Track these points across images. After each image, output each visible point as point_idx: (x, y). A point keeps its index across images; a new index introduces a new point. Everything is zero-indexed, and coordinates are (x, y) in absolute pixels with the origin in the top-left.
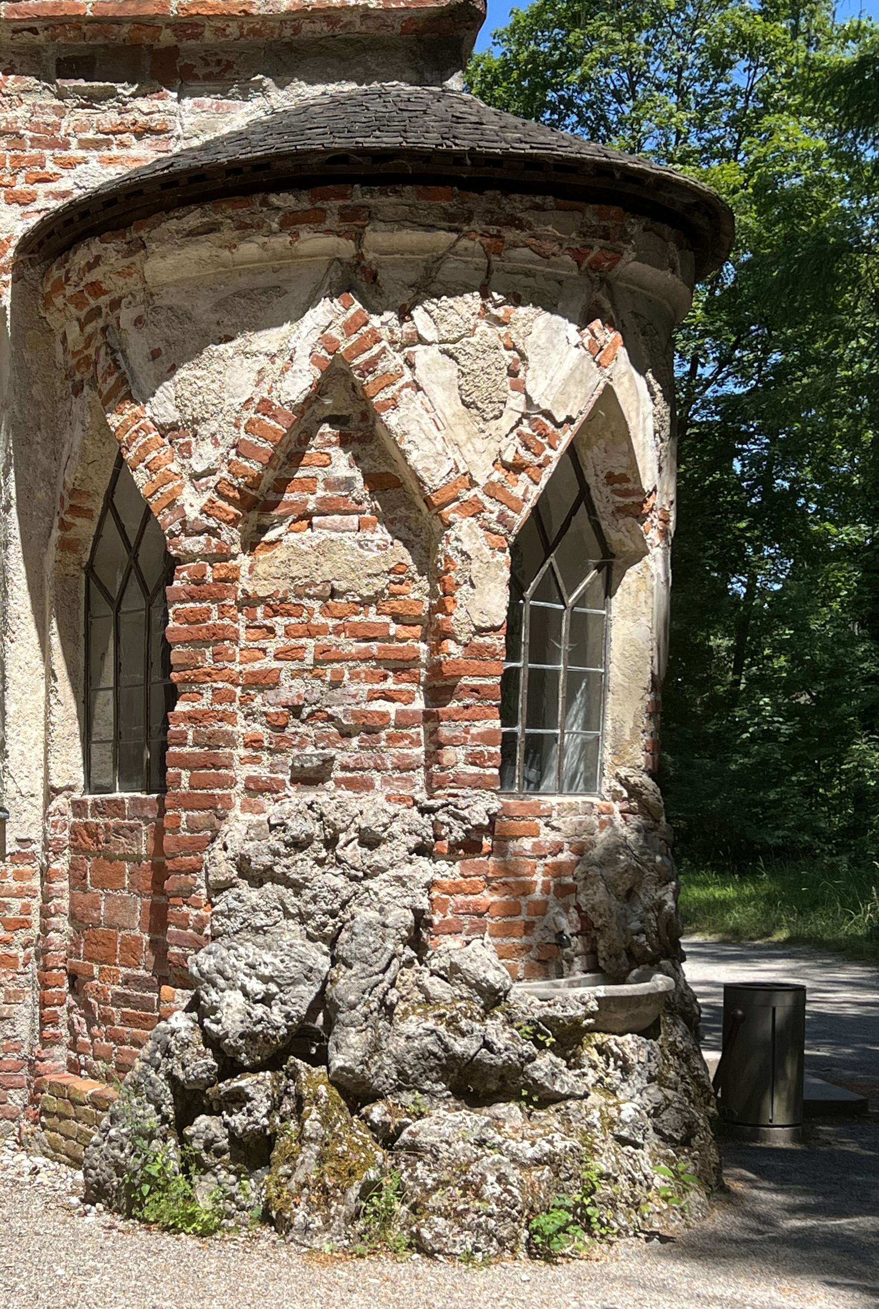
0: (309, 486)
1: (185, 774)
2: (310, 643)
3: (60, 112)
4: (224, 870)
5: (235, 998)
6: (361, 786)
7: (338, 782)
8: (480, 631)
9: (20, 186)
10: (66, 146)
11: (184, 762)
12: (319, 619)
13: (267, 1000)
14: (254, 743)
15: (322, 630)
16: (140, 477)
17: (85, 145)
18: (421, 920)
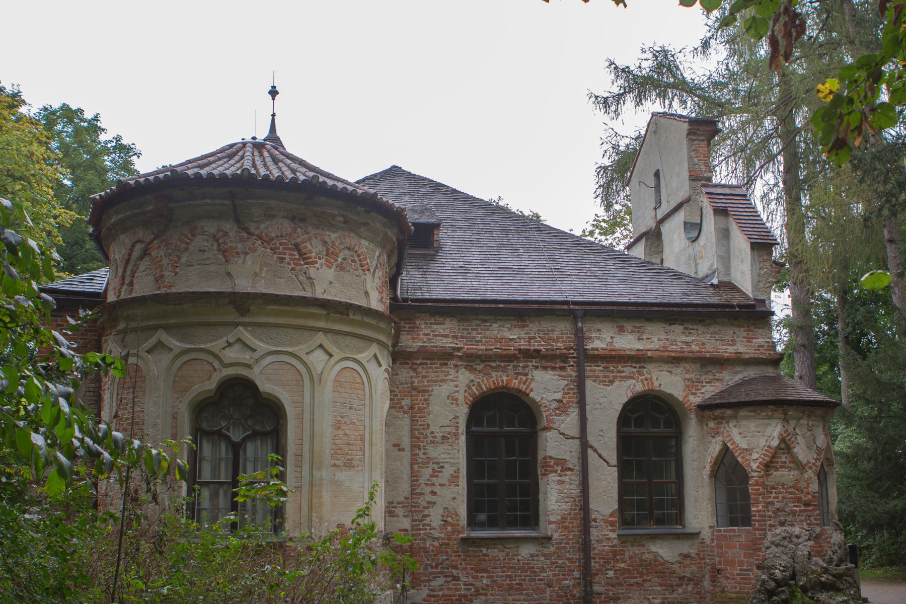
0: (777, 462)
1: (757, 524)
2: (780, 495)
3: (701, 375)
4: (768, 544)
5: (777, 571)
6: (793, 525)
7: (788, 525)
8: (814, 493)
9: (693, 391)
11: (756, 521)
12: (782, 490)
13: (784, 571)
14: (770, 516)
16: (739, 459)
17: (706, 382)
18: (810, 554)
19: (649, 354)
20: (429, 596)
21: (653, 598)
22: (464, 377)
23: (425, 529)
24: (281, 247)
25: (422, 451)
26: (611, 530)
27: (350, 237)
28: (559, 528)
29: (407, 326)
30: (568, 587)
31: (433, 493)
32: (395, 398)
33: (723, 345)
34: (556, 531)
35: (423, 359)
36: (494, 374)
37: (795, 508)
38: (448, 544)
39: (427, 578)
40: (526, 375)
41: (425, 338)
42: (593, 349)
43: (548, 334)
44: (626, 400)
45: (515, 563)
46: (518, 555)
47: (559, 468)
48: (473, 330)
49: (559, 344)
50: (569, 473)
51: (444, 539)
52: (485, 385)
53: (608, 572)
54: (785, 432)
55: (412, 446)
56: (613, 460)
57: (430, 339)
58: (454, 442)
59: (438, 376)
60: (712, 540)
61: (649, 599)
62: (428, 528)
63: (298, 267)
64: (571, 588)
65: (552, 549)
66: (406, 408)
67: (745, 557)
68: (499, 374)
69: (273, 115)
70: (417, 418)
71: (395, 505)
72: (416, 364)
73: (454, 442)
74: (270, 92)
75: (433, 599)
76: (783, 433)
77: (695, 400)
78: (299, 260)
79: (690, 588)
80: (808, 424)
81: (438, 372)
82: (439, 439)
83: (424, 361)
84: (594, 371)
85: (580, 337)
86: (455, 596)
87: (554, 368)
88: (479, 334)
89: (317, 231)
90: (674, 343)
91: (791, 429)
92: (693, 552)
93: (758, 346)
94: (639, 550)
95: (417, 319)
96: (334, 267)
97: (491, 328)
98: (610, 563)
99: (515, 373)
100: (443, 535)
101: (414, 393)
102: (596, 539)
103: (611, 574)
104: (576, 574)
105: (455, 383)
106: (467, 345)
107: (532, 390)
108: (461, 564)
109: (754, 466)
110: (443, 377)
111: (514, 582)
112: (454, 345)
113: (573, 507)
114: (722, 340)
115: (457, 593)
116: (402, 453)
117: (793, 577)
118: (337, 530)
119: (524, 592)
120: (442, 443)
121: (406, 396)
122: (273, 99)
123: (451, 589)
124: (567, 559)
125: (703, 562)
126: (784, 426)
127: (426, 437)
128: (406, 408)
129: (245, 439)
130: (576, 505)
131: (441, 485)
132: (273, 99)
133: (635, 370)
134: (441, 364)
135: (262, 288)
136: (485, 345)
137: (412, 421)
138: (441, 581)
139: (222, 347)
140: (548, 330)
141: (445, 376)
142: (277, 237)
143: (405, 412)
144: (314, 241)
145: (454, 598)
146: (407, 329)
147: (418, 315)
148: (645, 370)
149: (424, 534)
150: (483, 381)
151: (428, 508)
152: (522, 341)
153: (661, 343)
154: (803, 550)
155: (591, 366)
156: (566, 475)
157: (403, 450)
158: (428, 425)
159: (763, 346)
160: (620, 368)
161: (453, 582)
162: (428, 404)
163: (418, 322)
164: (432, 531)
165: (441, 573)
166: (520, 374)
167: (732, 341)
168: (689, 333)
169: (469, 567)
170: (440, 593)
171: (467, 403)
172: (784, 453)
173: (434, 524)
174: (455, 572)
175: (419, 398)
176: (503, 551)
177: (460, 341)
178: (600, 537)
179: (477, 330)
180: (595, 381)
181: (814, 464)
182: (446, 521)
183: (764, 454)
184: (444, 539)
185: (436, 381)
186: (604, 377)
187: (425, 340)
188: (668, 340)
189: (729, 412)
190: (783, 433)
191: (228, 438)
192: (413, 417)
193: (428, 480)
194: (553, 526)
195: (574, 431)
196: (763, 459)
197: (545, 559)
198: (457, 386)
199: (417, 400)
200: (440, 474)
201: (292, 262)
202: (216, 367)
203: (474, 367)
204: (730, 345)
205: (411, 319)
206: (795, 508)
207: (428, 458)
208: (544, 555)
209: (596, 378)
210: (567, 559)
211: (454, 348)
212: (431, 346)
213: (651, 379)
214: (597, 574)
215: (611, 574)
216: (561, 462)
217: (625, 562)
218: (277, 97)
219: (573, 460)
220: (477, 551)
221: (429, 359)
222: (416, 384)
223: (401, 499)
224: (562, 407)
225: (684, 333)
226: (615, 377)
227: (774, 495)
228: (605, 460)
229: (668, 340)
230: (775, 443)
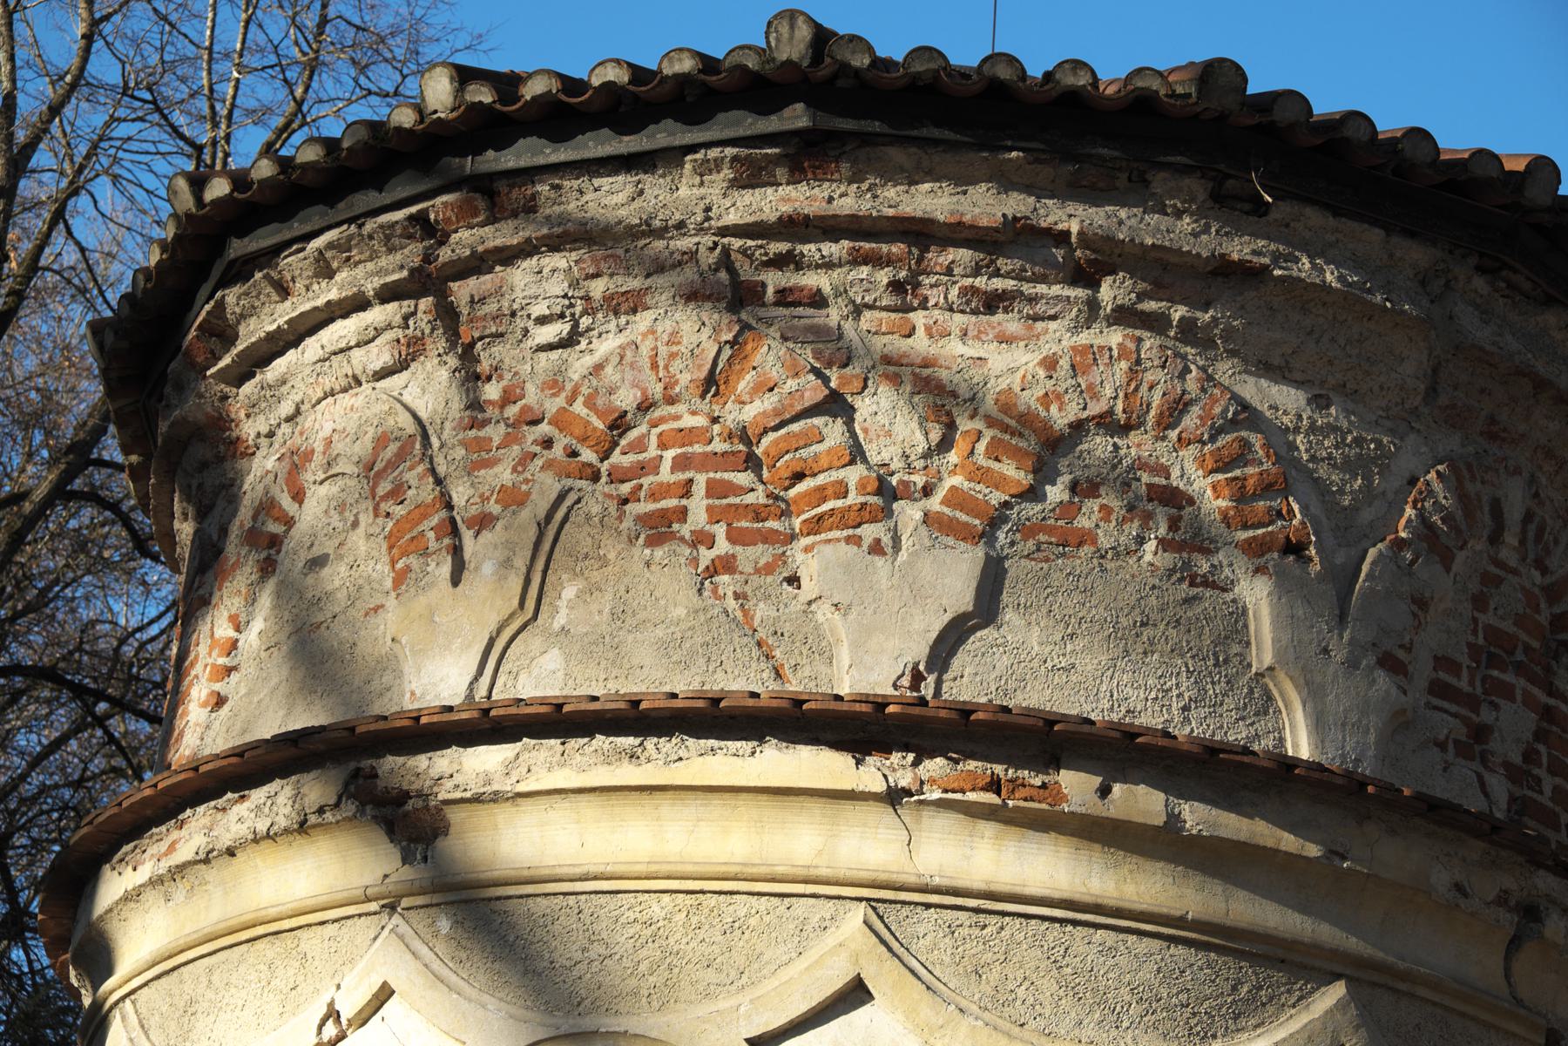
63: (749, 556)
142: (645, 407)
201: (720, 530)
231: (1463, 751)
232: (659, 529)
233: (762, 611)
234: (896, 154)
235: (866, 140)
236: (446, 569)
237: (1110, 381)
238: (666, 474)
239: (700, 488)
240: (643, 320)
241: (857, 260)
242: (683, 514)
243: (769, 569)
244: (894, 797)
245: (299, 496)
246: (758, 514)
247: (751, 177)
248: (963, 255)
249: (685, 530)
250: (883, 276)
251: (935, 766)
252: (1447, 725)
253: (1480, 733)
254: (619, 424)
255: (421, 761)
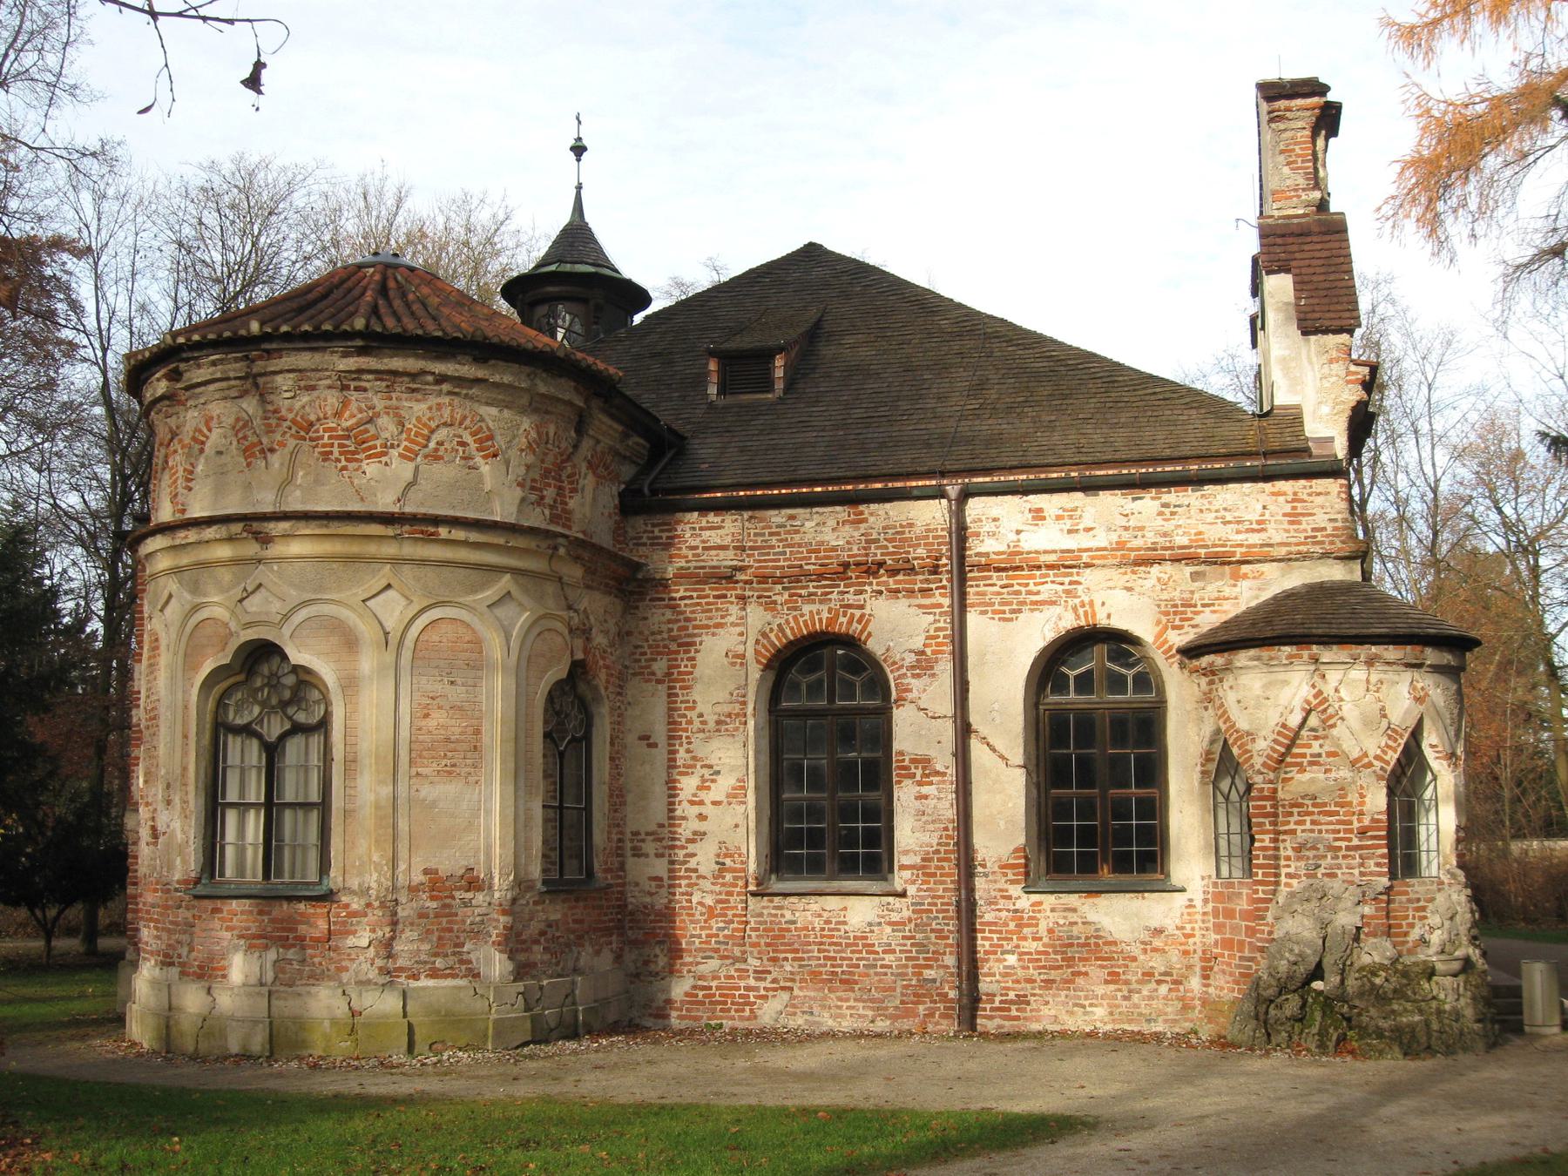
1: (1260, 872)
2: (1308, 819)
9: (1177, 623)
10: (1195, 606)
12: (1311, 809)
14: (1288, 858)
15: (1313, 813)
19: (1085, 557)
20: (695, 987)
21: (1091, 1005)
22: (756, 616)
23: (690, 878)
24: (326, 435)
25: (685, 746)
26: (1013, 882)
27: (450, 404)
28: (918, 876)
29: (664, 535)
30: (934, 981)
31: (702, 817)
32: (643, 658)
33: (1238, 532)
34: (913, 882)
35: (686, 590)
36: (806, 609)
37: (1337, 844)
38: (728, 901)
39: (691, 960)
40: (862, 607)
41: (690, 553)
42: (977, 554)
43: (903, 533)
44: (1041, 644)
45: (841, 937)
46: (845, 923)
47: (919, 773)
48: (771, 534)
49: (919, 551)
50: (935, 779)
51: (720, 893)
52: (792, 629)
53: (1006, 956)
54: (1316, 696)
55: (671, 738)
56: (1017, 756)
57: (698, 555)
58: (736, 729)
59: (710, 618)
60: (1206, 901)
61: (1084, 1007)
62: (694, 875)
63: (352, 466)
64: (938, 984)
65: (906, 914)
66: (659, 674)
67: (1247, 936)
68: (814, 608)
69: (579, 187)
70: (677, 691)
71: (643, 836)
72: (675, 599)
73: (736, 729)
74: (584, 149)
75: (701, 993)
76: (1311, 698)
77: (1178, 639)
78: (353, 453)
79: (1163, 989)
80: (1368, 681)
81: (711, 610)
82: (711, 725)
83: (688, 594)
84: (984, 594)
85: (961, 533)
86: (738, 988)
87: (911, 593)
88: (781, 541)
89: (389, 403)
90: (1140, 534)
91: (1328, 690)
92: (1170, 924)
93: (1313, 530)
94: (1065, 918)
95: (679, 522)
96: (419, 459)
97: (802, 529)
98: (1012, 939)
99: (841, 606)
100: (717, 888)
101: (674, 647)
102: (985, 895)
103: (1012, 959)
104: (950, 960)
105: (739, 629)
106: (760, 561)
107: (870, 635)
108: (750, 936)
109: (1258, 762)
110: (719, 620)
111: (839, 970)
112: (735, 563)
113: (944, 840)
114: (1238, 522)
115: (742, 984)
116: (654, 751)
117: (1318, 973)
118: (422, 878)
119: (857, 987)
120: (718, 730)
121: (659, 653)
122: (579, 160)
123: (732, 977)
124: (933, 931)
125: (1191, 941)
126: (1313, 686)
127: (690, 722)
128: (659, 674)
129: (283, 737)
130: (948, 837)
131: (715, 803)
132: (579, 160)
133: (1060, 588)
134: (716, 597)
135: (295, 503)
136: (790, 559)
137: (669, 695)
138: (714, 964)
139: (239, 597)
140: (901, 526)
141: (723, 617)
142: (319, 419)
143: (659, 682)
144: (384, 421)
145: (737, 993)
146: (664, 540)
147: (679, 515)
148: (1080, 588)
149: (688, 885)
150: (787, 622)
151: (693, 841)
152: (855, 548)
153: (1114, 537)
154: (1346, 919)
155: (977, 586)
156: (931, 783)
157: (655, 745)
158: (694, 702)
159: (1324, 529)
160: (1032, 587)
161: (738, 966)
162: (694, 666)
163: (679, 528)
164: (701, 881)
165: (716, 951)
166: (849, 606)
167: (1259, 522)
168: (1172, 514)
169: (762, 941)
170: (714, 984)
171: (758, 662)
172: (1316, 738)
173: (703, 870)
174: (737, 951)
175: (679, 657)
176: (820, 916)
177: (748, 556)
178: (993, 894)
179: (778, 534)
180: (984, 613)
181: (1377, 757)
182: (724, 864)
183: (1275, 741)
184: (720, 893)
185: (708, 627)
186: (1002, 604)
187: (690, 558)
188: (1126, 529)
189: (1218, 660)
190: (1311, 698)
191: (259, 736)
192: (670, 688)
193: (695, 795)
194: (907, 874)
195: (946, 707)
196: (1274, 750)
197: (893, 931)
198: (741, 634)
199: (676, 660)
200: (712, 785)
201: (343, 458)
202: (233, 629)
203: (774, 598)
204: (1253, 531)
205: (669, 524)
206: (1337, 844)
207: (694, 758)
208: (890, 923)
209: (985, 607)
210: (933, 931)
211: (736, 569)
212: (696, 568)
213: (1091, 603)
214: (987, 960)
215: (1012, 959)
216: (925, 762)
217: (1040, 939)
218: (585, 156)
219: (944, 761)
220: (776, 915)
221: (695, 590)
222: (675, 633)
223: (653, 827)
224: (923, 665)
225: (1160, 514)
226: (1023, 603)
227: (1296, 818)
228: (1002, 757)
229: (1126, 529)
230: (1294, 720)
231: (539, 504)
232: (326, 456)
233: (356, 482)
234: (386, 351)
235: (378, 348)
236: (264, 464)
237: (446, 412)
238: (326, 440)
239: (336, 445)
240: (315, 394)
241: (377, 380)
242: (331, 453)
243: (357, 470)
244: (394, 537)
245: (210, 430)
246: (353, 453)
247: (345, 355)
248: (406, 379)
249: (333, 457)
250: (384, 384)
251: (407, 528)
252: (533, 497)
253: (542, 498)
254: (311, 424)
255: (266, 524)
